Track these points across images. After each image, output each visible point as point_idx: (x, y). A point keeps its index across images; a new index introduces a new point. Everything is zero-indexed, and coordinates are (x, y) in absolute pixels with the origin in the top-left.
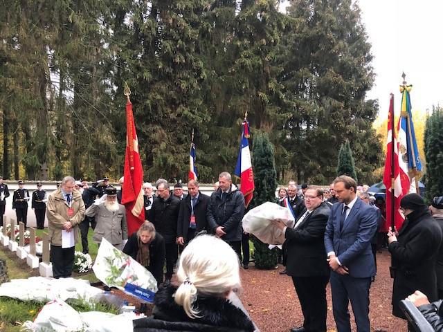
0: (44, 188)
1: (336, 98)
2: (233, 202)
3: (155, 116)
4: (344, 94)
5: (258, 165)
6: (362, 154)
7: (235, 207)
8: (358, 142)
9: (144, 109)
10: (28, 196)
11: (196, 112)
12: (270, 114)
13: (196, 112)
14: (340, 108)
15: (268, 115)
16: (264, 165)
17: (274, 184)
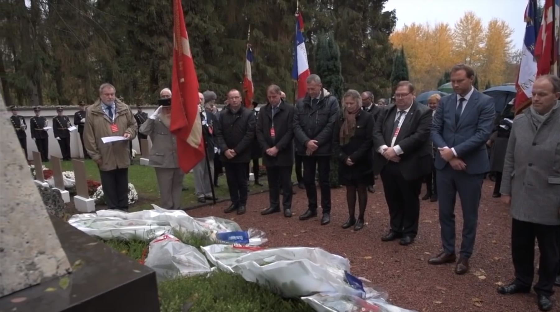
0: (42, 114)
1: (353, 8)
2: (326, 109)
3: (161, 26)
4: (362, 3)
5: (324, 71)
6: (380, 69)
7: (329, 116)
8: (376, 56)
9: (148, 17)
10: (25, 123)
11: (208, 21)
12: (289, 24)
13: (208, 21)
14: (358, 20)
15: (286, 26)
16: (329, 70)
17: (341, 93)
